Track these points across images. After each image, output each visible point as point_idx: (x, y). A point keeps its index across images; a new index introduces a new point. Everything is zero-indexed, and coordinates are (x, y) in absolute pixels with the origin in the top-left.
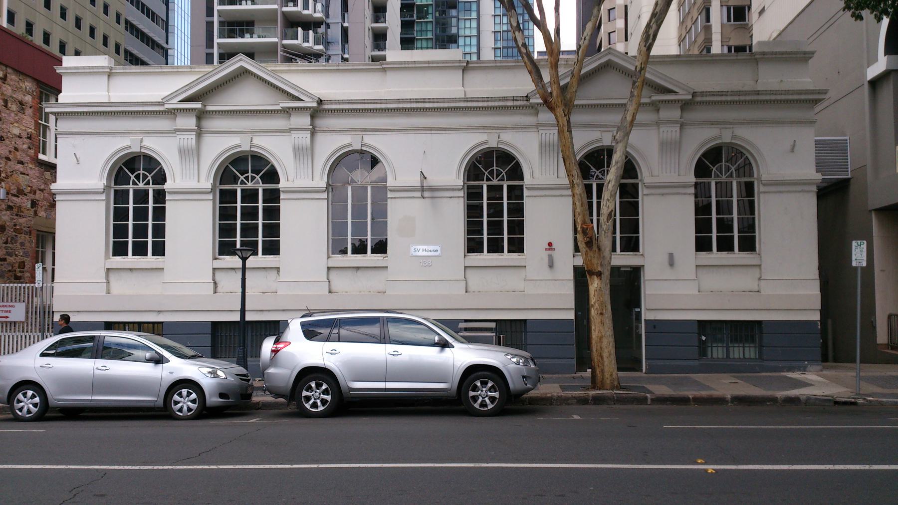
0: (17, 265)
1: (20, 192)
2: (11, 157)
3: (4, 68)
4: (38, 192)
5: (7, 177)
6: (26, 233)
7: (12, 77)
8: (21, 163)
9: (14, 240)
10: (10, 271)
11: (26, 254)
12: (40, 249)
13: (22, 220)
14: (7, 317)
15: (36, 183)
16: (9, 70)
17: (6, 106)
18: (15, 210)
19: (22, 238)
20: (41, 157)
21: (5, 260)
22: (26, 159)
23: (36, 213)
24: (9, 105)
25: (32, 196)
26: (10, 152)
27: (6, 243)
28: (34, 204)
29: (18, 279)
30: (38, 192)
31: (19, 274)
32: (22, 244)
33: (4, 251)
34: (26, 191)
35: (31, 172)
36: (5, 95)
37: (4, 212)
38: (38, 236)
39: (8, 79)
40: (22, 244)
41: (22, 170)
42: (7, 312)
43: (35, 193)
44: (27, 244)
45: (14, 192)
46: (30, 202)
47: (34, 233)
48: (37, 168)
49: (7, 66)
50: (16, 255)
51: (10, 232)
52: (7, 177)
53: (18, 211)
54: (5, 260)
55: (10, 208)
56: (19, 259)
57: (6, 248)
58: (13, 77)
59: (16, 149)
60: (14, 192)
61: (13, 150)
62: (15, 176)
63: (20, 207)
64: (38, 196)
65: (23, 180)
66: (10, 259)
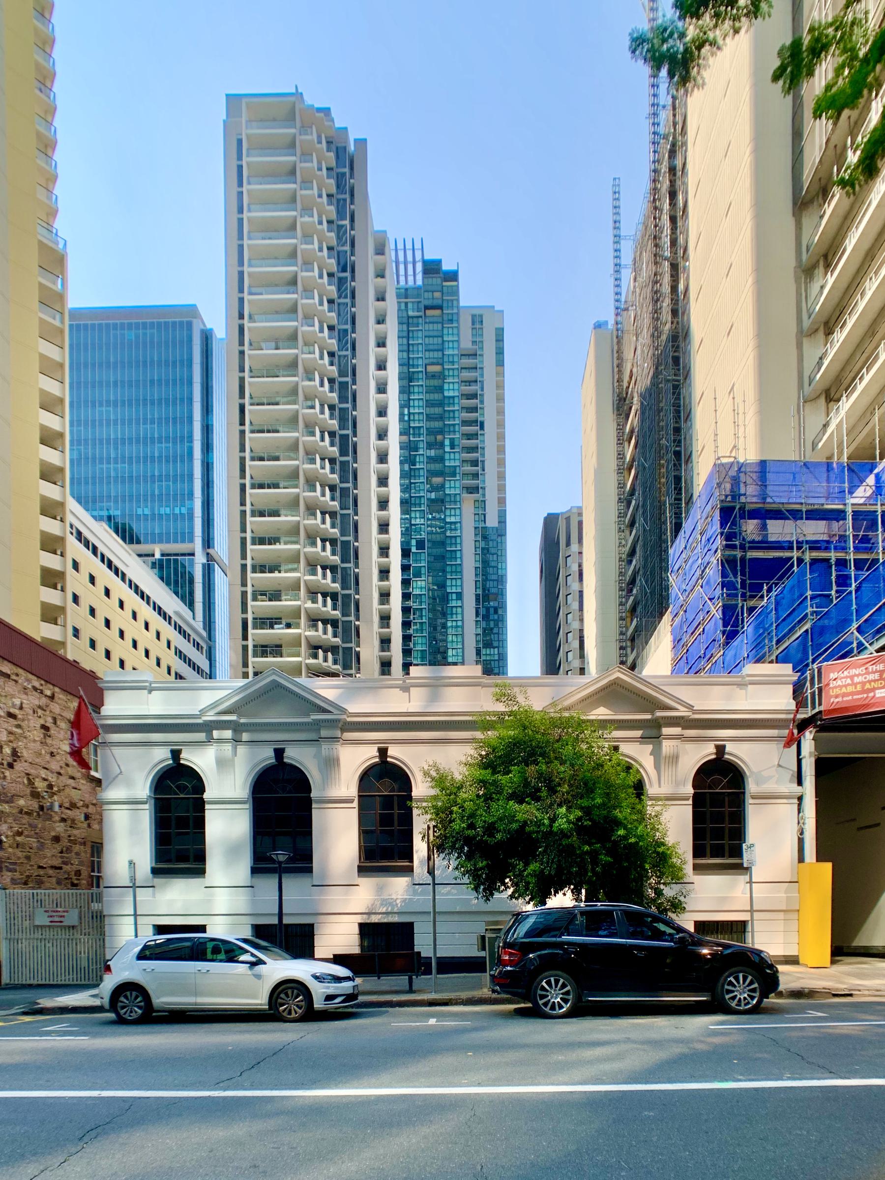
0: (73, 873)
1: (73, 806)
2: (62, 772)
3: (51, 687)
4: (91, 806)
5: (59, 791)
6: (81, 844)
7: (60, 696)
8: (73, 778)
9: (69, 850)
10: (66, 879)
11: (81, 863)
12: (96, 859)
13: (75, 832)
14: (61, 922)
15: (88, 798)
16: (57, 690)
17: (55, 723)
18: (69, 822)
19: (77, 848)
20: (93, 773)
21: (60, 868)
22: (78, 775)
23: (89, 826)
24: (58, 723)
25: (85, 810)
26: (61, 767)
27: (61, 852)
28: (87, 817)
29: (74, 885)
30: (91, 806)
31: (76, 882)
32: (77, 854)
33: (60, 860)
34: (78, 805)
35: (81, 787)
36: (54, 713)
37: (58, 824)
38: (92, 847)
39: (56, 699)
40: (77, 854)
41: (74, 785)
42: (61, 916)
43: (87, 807)
44: (83, 854)
45: (67, 805)
46: (83, 816)
47: (89, 844)
48: (89, 784)
49: (54, 685)
50: (72, 864)
51: (65, 843)
52: (59, 791)
53: (73, 824)
54: (60, 868)
55: (63, 820)
56: (75, 868)
57: (62, 857)
58: (61, 696)
59: (67, 765)
60: (67, 805)
61: (64, 765)
62: (67, 790)
63: (73, 821)
64: (91, 809)
65: (75, 795)
66: (67, 868)
